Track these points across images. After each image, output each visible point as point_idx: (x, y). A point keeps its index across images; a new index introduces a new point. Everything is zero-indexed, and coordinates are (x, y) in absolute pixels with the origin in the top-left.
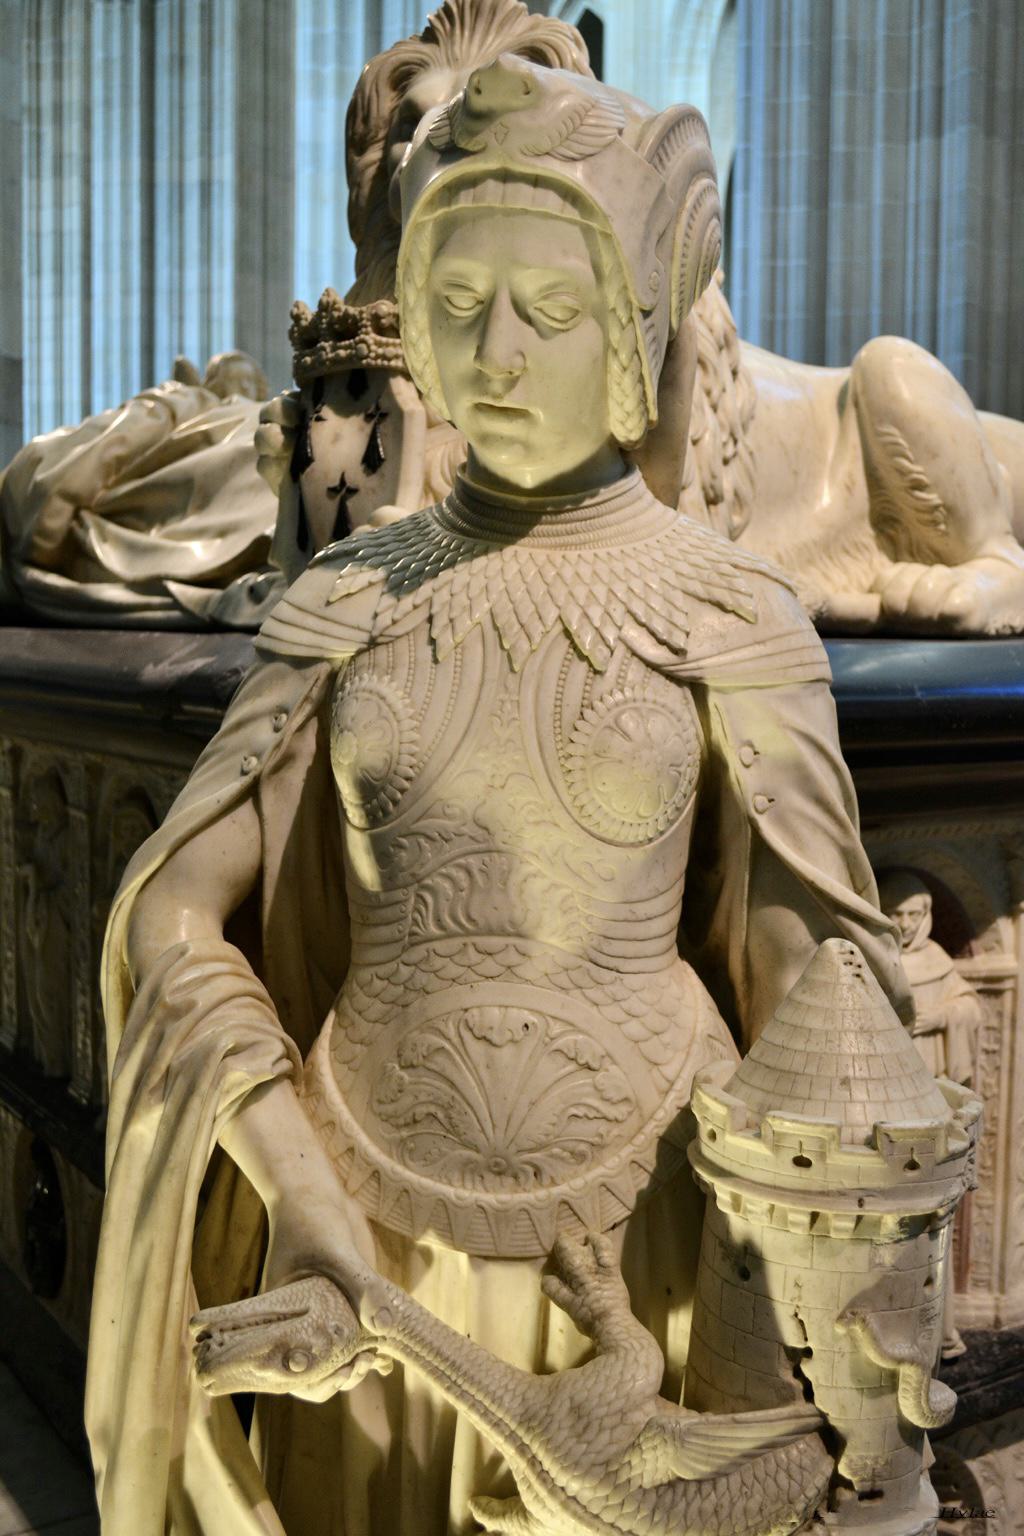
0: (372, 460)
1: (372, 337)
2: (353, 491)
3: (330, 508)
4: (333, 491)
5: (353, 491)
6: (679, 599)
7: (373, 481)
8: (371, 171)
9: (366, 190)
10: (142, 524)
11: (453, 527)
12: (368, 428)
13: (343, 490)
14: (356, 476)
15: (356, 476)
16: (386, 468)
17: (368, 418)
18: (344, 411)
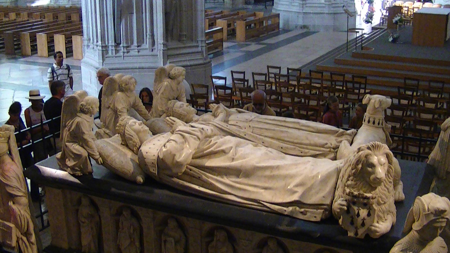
0: (369, 215)
1: (371, 200)
2: (365, 219)
3: (361, 222)
4: (362, 220)
5: (365, 219)
6: (440, 248)
7: (369, 218)
8: (360, 168)
9: (359, 171)
10: (216, 174)
11: (418, 244)
12: (368, 211)
13: (364, 219)
14: (366, 217)
15: (366, 217)
16: (372, 217)
17: (367, 209)
18: (363, 208)
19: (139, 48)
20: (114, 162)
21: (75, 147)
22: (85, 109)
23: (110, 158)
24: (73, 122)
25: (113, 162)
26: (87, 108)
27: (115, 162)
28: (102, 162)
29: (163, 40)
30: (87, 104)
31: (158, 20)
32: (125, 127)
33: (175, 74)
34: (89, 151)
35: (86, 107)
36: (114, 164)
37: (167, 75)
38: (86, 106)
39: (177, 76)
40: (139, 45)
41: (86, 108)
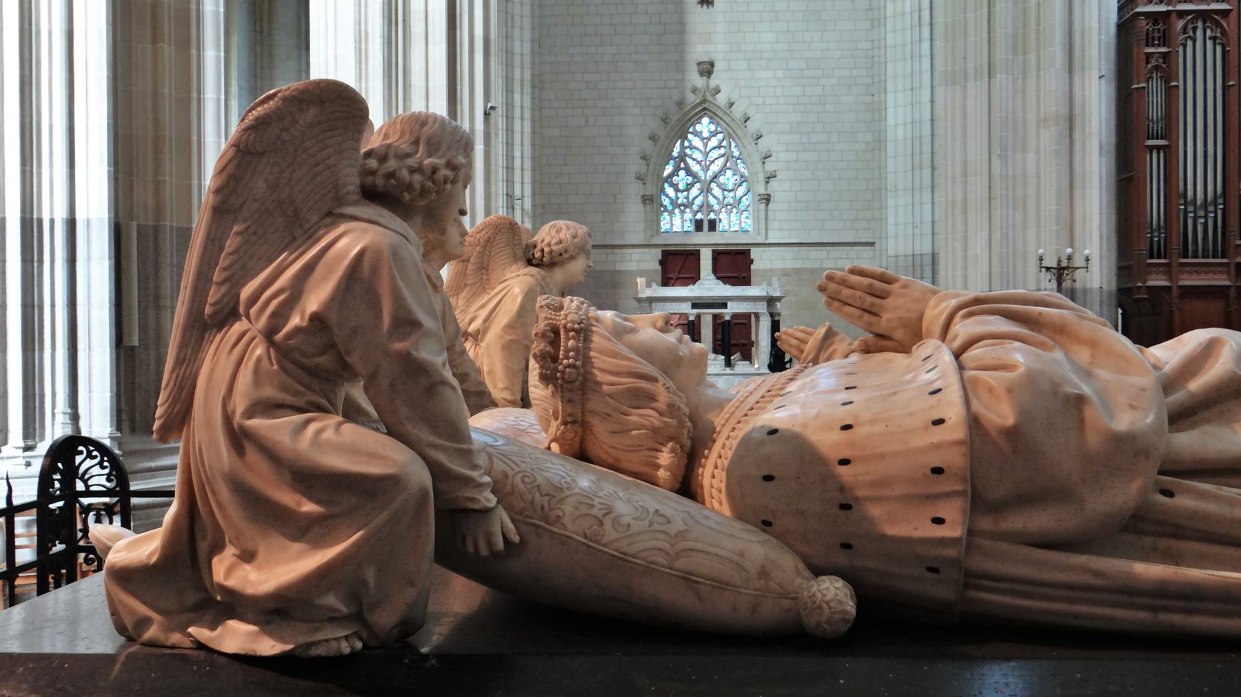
19: (28, 453)
20: (608, 522)
21: (329, 434)
22: (405, 174)
23: (571, 500)
24: (309, 269)
25: (601, 523)
26: (418, 169)
27: (616, 521)
28: (516, 539)
29: (111, 427)
30: (416, 142)
31: (95, 371)
32: (587, 340)
33: (560, 242)
34: (442, 457)
35: (411, 162)
36: (610, 533)
37: (520, 252)
38: (408, 155)
39: (571, 249)
40: (30, 443)
41: (412, 171)
